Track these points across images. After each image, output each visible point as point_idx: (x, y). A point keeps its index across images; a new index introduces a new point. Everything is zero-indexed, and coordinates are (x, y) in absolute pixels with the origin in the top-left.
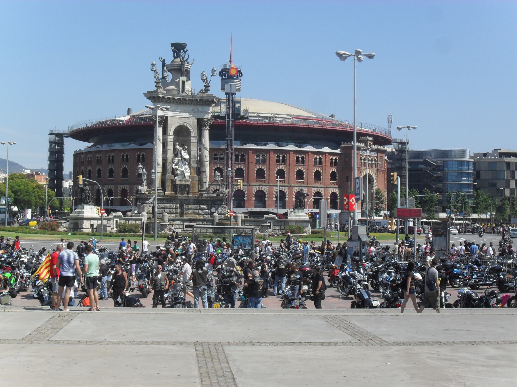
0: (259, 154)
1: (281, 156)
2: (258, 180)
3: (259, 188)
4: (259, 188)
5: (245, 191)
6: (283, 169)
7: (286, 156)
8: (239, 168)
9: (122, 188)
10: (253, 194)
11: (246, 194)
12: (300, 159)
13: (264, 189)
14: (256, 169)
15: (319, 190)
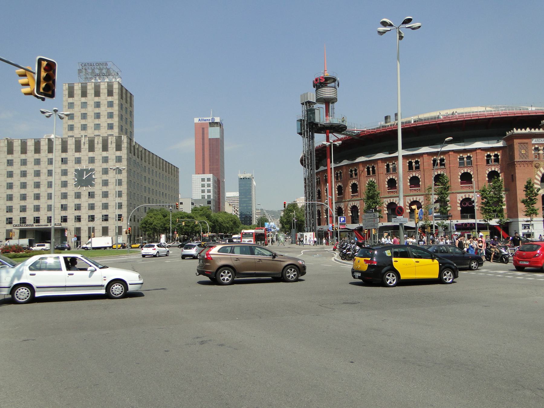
0: (389, 163)
1: (413, 161)
2: (390, 191)
3: (390, 200)
4: (413, 198)
5: (422, 202)
6: (394, 178)
7: (419, 160)
8: (411, 178)
9: (338, 207)
10: (458, 203)
11: (359, 209)
12: (414, 164)
13: (396, 201)
14: (387, 180)
15: (469, 195)
